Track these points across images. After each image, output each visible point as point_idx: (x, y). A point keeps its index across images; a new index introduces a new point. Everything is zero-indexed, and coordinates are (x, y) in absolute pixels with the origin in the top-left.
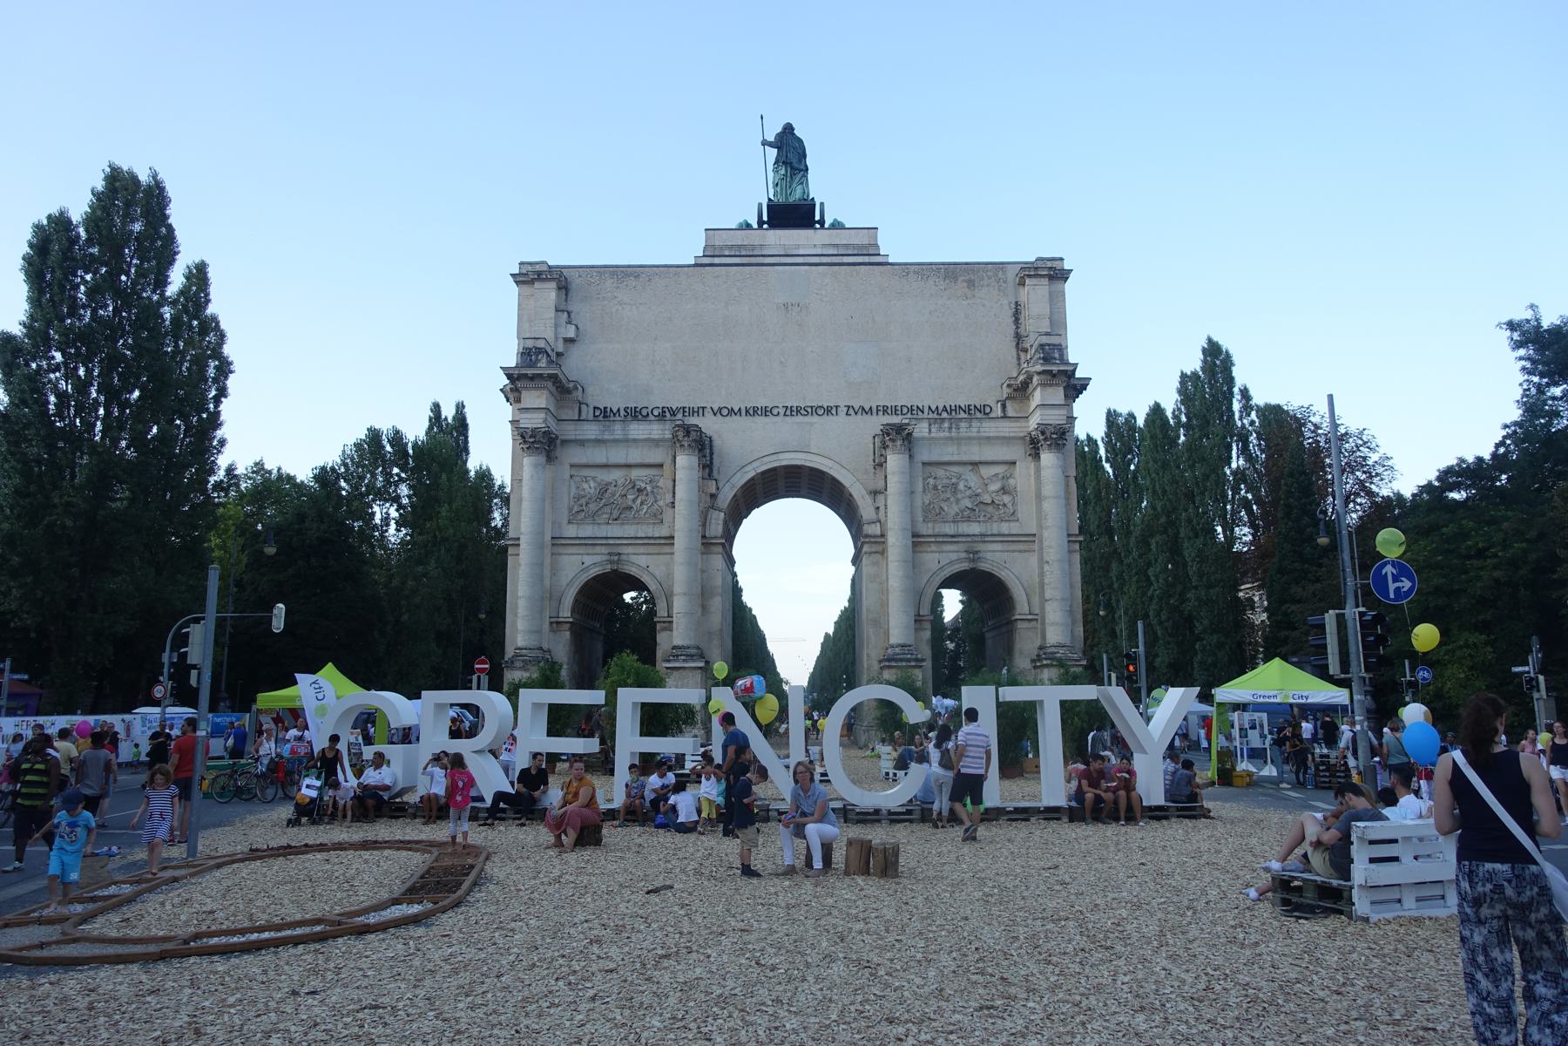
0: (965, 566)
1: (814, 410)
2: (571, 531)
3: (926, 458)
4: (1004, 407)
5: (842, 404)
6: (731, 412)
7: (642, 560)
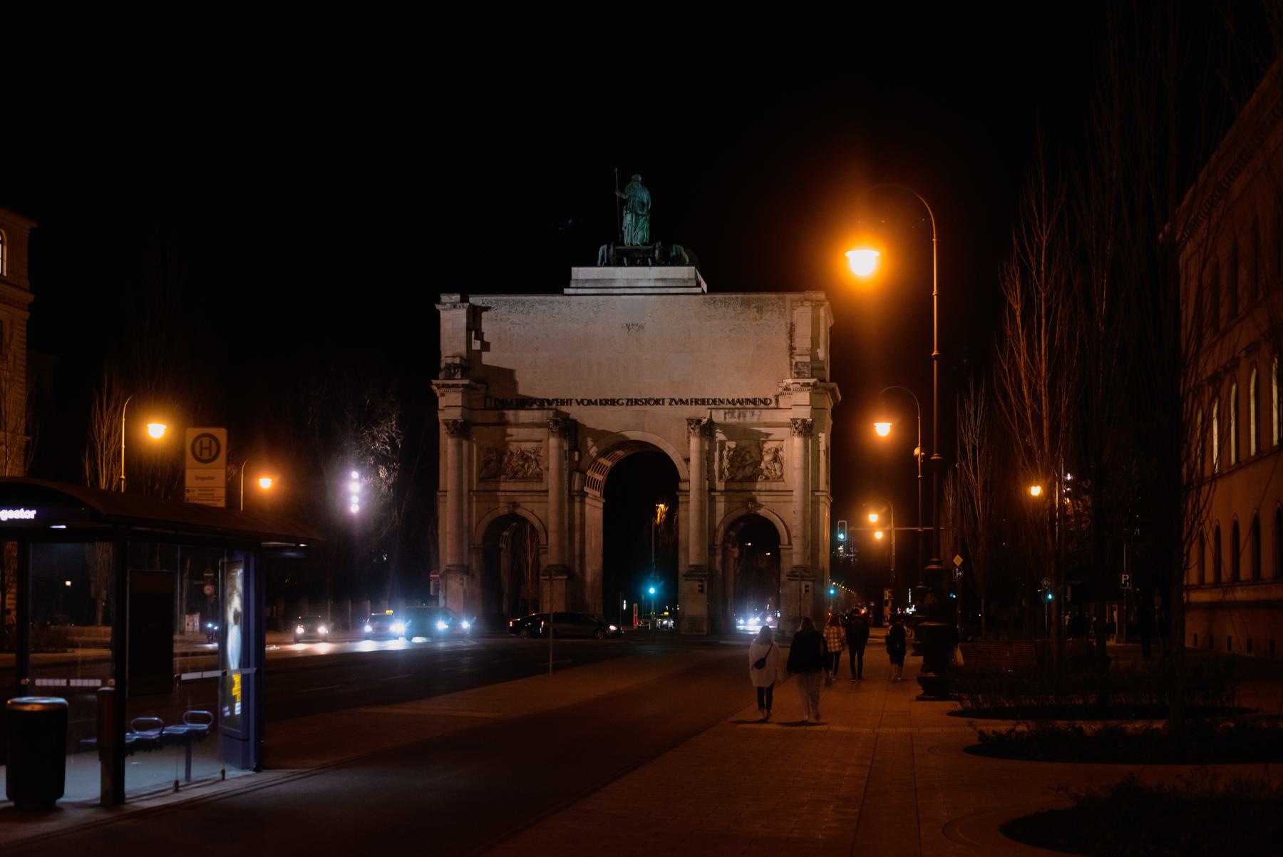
1: (647, 402)
4: (777, 401)
6: (590, 402)
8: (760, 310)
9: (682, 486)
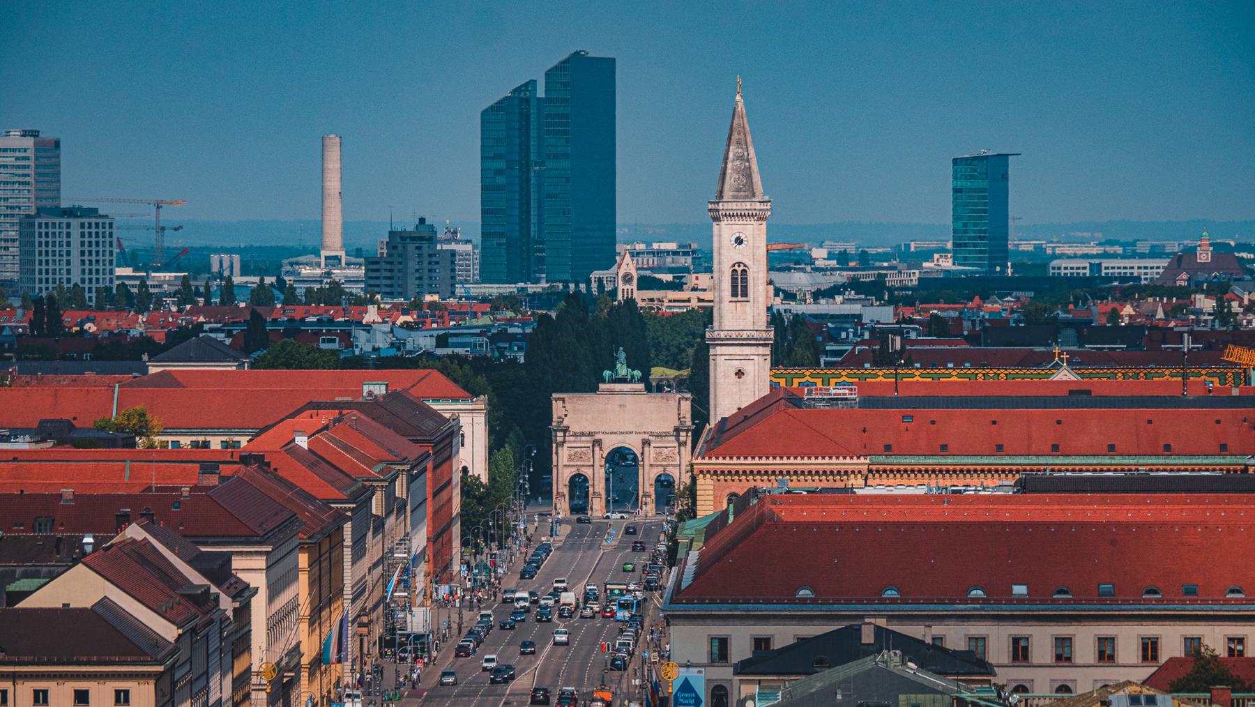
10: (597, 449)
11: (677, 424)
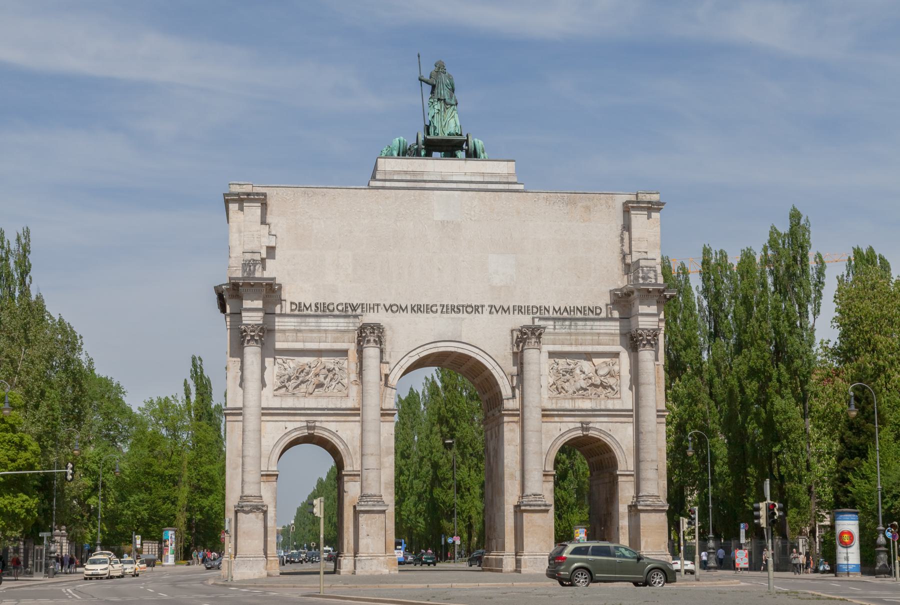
0: (579, 433)
2: (276, 403)
3: (552, 348)
5: (487, 305)
6: (401, 309)
7: (332, 427)
8: (588, 208)
9: (509, 404)
10: (371, 352)
11: (620, 282)
